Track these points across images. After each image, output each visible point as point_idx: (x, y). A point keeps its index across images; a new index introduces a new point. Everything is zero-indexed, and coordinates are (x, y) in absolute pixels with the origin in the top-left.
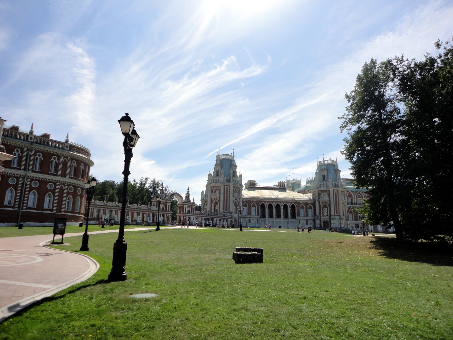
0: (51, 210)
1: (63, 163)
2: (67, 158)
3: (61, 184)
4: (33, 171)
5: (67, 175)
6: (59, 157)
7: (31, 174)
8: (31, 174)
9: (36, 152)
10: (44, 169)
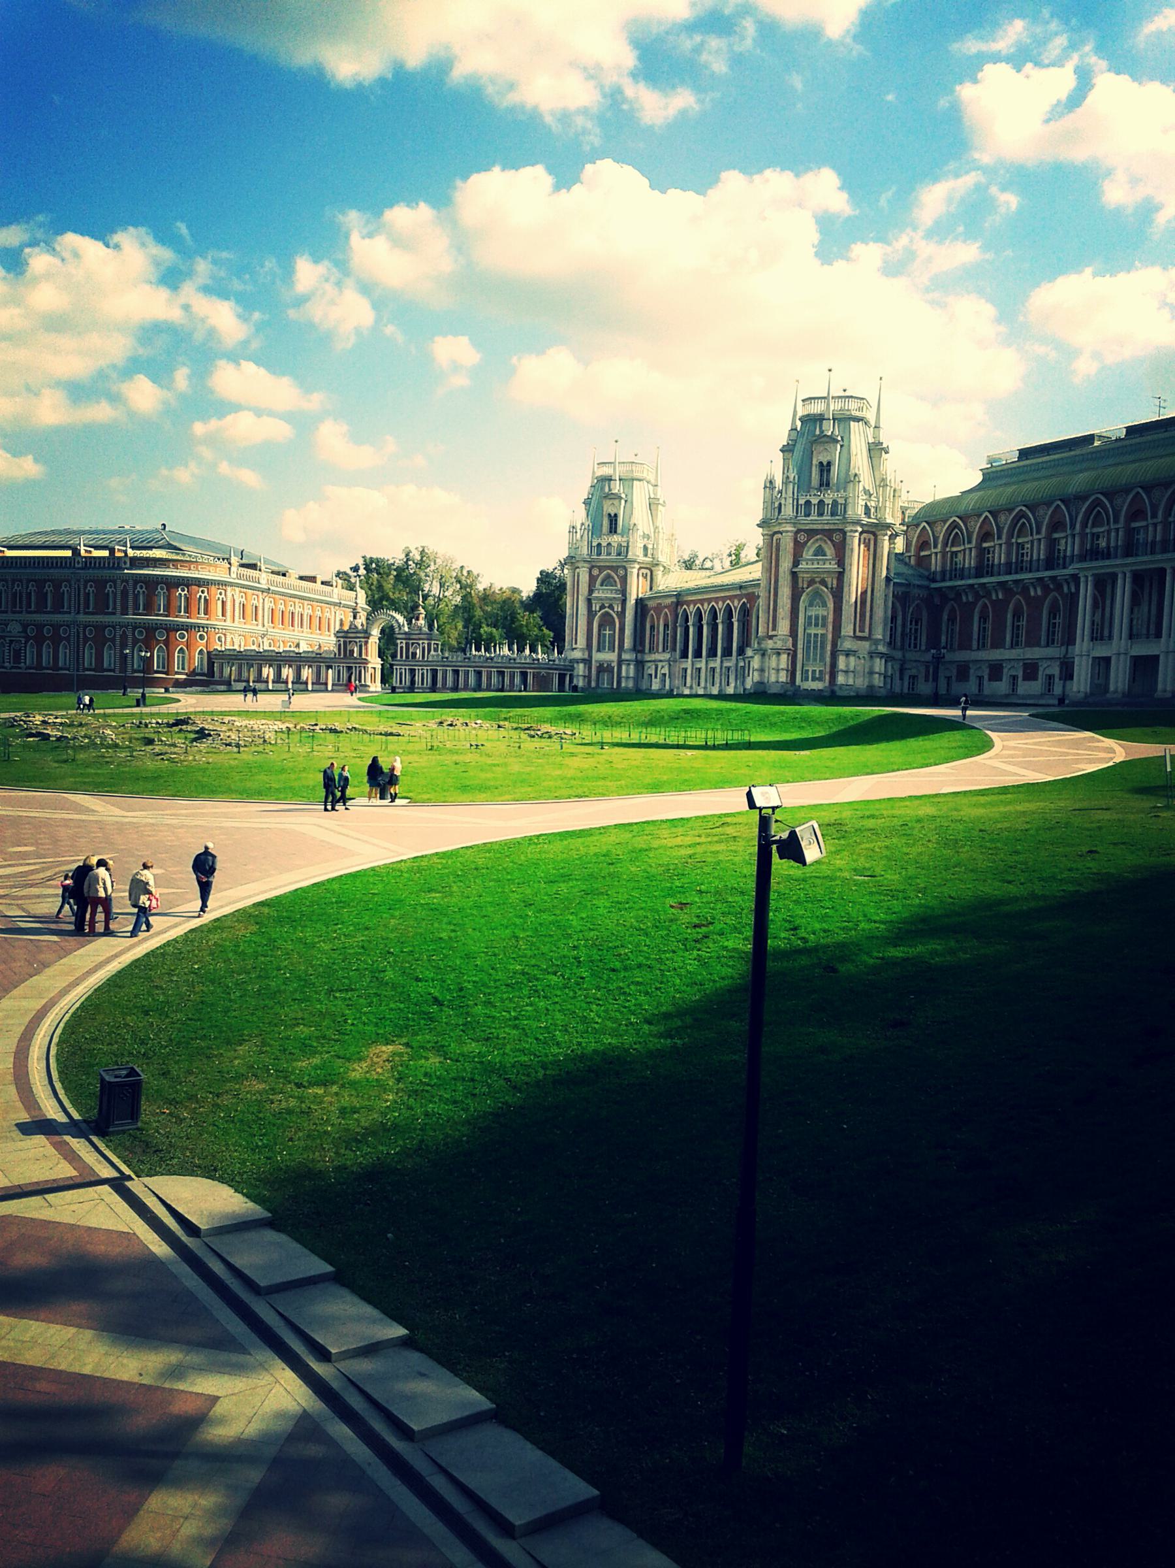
0: (113, 671)
1: (122, 592)
2: (127, 581)
3: (121, 627)
4: (86, 613)
5: (130, 611)
6: (114, 582)
7: (82, 618)
8: (82, 618)
9: (86, 582)
10: (103, 606)
